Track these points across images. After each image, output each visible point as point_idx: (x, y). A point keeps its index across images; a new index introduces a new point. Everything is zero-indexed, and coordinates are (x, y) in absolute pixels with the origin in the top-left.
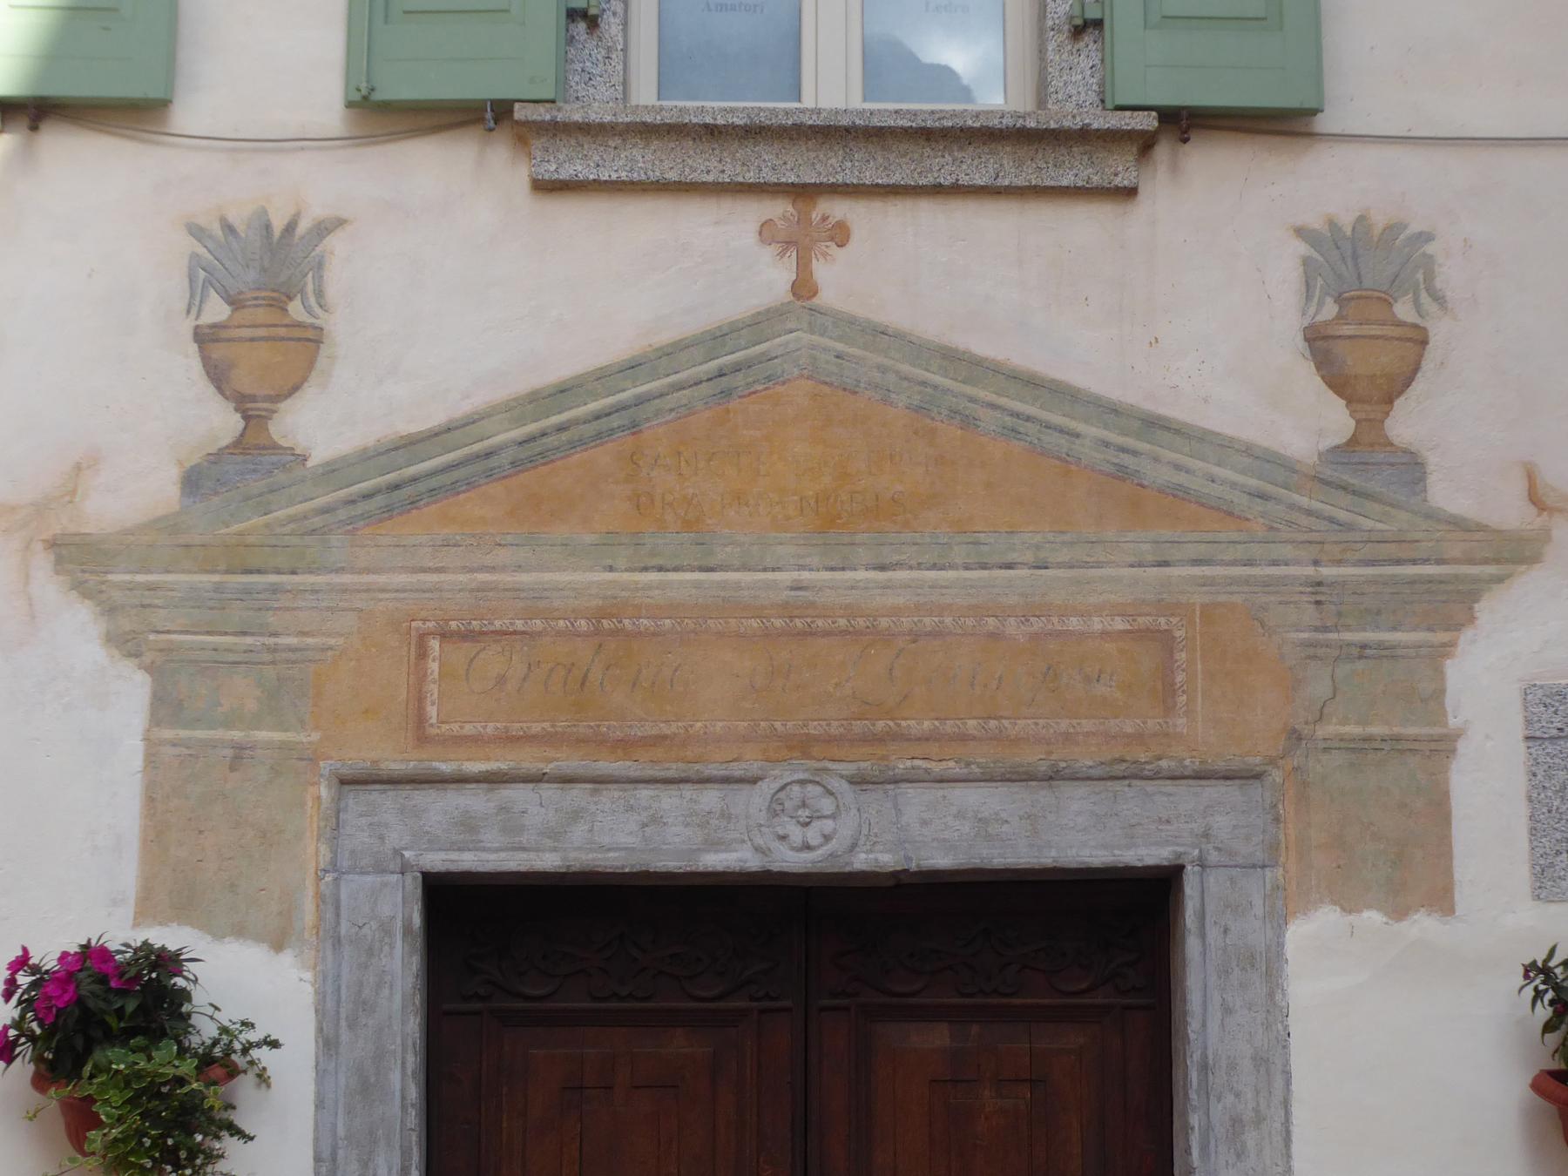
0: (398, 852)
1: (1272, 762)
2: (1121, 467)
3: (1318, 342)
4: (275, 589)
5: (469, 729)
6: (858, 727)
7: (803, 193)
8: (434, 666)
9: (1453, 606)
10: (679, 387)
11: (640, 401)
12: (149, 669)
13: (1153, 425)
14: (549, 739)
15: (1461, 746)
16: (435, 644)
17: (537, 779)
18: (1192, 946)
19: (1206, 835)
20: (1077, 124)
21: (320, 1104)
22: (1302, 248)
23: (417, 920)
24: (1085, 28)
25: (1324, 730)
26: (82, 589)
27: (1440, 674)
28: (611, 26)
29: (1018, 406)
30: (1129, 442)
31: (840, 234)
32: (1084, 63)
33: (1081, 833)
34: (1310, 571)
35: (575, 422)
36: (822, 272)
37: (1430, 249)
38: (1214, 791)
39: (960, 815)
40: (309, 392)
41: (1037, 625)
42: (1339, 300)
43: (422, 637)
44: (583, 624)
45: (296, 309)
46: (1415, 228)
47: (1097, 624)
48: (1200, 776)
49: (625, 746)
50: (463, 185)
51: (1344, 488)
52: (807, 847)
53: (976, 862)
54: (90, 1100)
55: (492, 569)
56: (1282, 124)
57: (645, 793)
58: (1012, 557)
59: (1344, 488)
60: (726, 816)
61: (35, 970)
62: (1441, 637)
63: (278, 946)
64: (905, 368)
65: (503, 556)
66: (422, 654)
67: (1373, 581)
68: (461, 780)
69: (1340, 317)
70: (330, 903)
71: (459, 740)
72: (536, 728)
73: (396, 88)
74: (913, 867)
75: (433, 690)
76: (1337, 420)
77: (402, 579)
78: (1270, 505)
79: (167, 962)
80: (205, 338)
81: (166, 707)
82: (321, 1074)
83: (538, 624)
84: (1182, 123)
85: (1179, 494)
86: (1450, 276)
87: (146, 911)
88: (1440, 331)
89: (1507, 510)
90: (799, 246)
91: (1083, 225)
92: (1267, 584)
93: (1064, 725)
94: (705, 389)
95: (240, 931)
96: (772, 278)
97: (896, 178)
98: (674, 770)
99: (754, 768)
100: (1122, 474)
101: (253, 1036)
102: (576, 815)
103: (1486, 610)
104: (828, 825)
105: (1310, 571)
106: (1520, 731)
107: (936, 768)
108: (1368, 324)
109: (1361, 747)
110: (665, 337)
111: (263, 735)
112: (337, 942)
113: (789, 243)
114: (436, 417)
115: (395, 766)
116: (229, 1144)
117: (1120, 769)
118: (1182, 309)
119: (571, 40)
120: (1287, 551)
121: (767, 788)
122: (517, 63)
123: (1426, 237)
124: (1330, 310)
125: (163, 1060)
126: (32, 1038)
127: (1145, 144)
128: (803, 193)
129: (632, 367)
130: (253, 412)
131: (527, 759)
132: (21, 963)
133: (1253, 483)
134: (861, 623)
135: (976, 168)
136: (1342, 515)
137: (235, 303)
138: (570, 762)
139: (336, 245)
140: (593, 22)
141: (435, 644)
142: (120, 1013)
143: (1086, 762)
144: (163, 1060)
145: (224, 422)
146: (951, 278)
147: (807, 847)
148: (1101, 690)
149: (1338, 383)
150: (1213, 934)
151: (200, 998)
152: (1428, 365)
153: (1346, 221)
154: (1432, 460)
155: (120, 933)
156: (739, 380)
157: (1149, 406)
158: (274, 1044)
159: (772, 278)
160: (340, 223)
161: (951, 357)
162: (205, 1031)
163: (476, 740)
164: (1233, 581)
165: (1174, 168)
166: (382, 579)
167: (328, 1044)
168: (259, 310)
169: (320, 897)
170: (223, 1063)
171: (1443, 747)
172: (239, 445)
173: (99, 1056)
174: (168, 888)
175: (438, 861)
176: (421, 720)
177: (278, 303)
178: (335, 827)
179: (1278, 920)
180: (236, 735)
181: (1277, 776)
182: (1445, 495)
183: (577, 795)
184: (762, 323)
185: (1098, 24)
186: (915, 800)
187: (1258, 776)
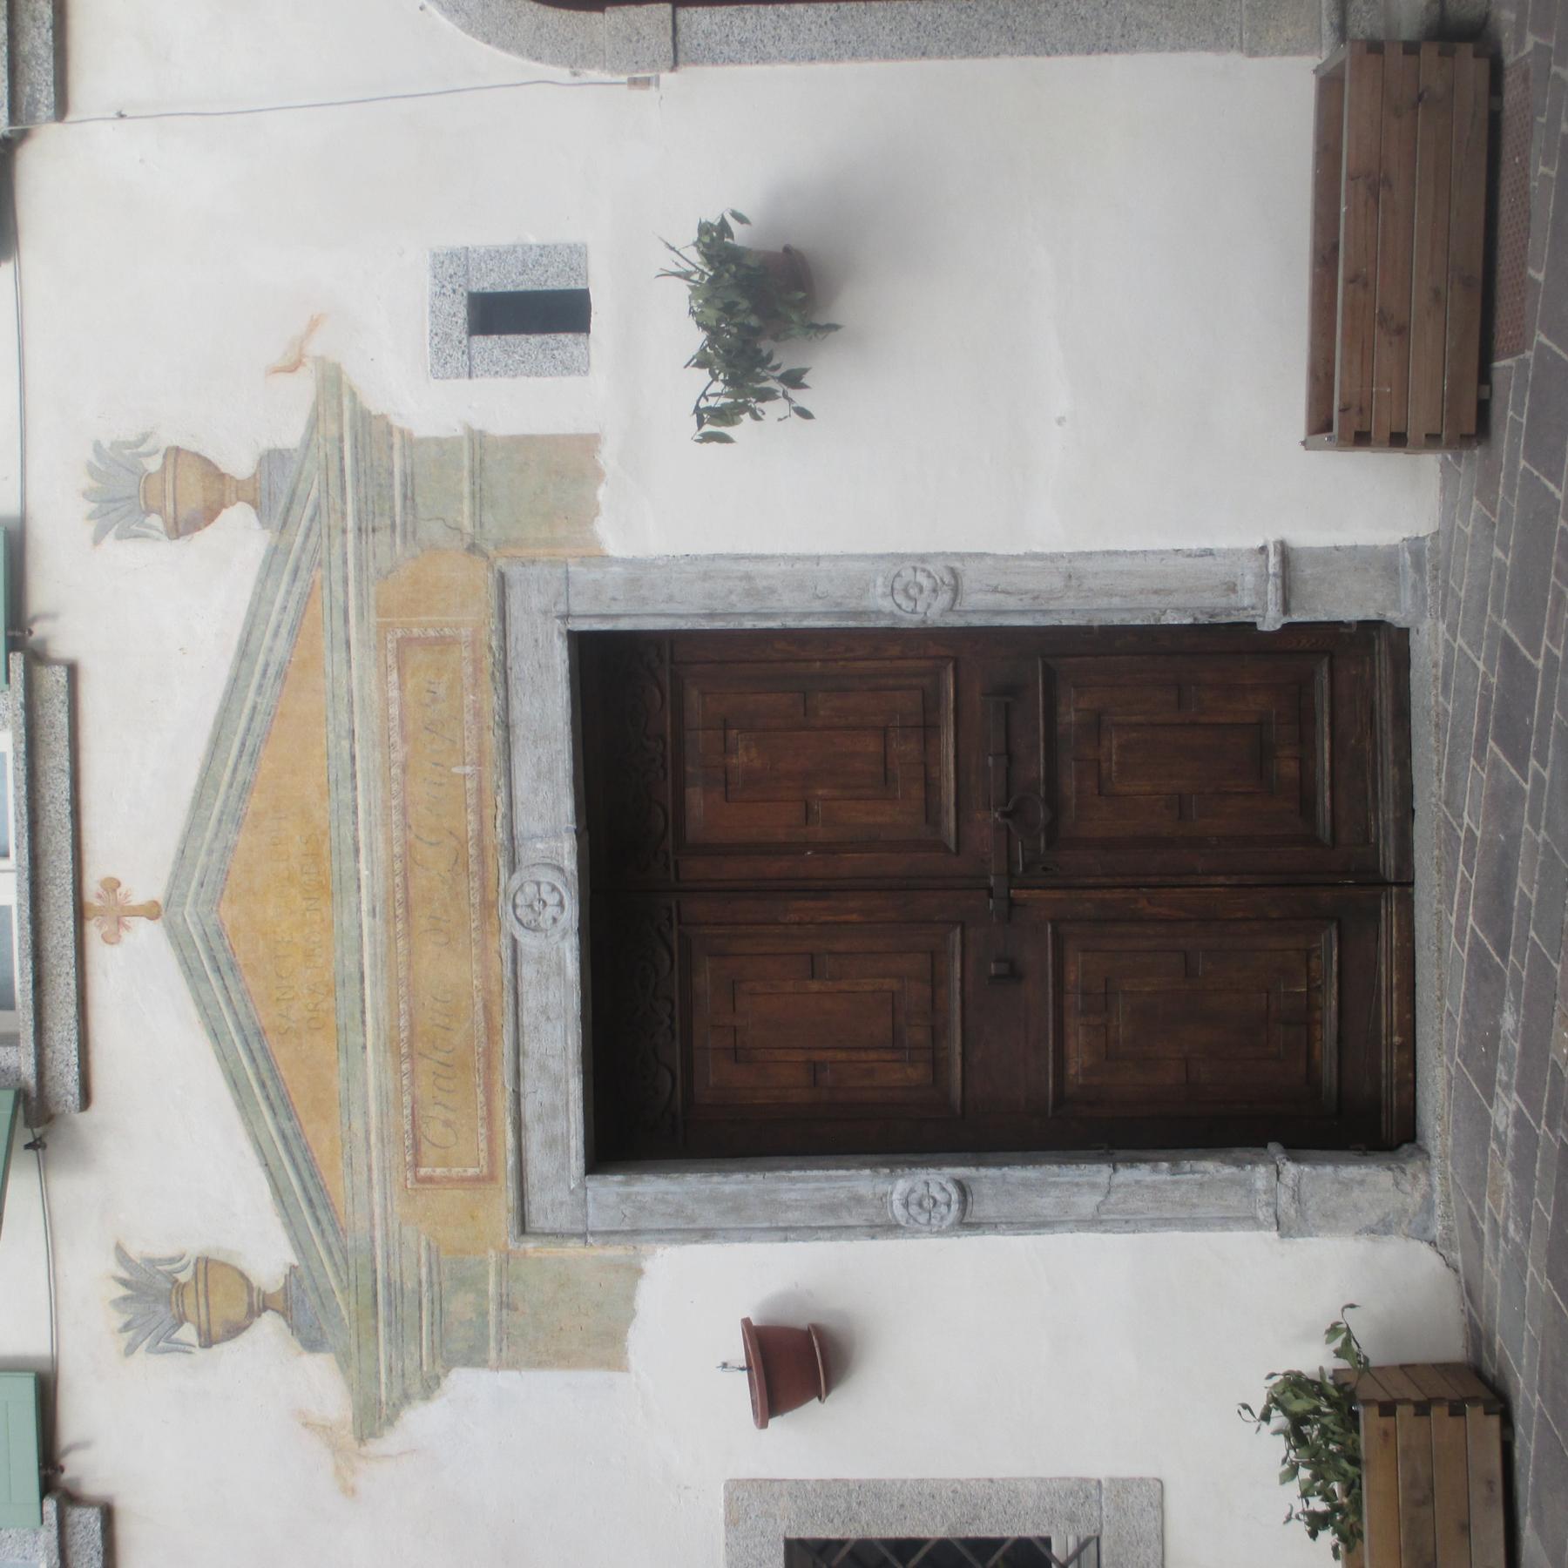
0: (572, 1192)
1: (491, 566)
2: (278, 674)
3: (180, 529)
5: (483, 1145)
6: (473, 867)
7: (80, 913)
8: (439, 1171)
9: (371, 432)
10: (229, 1001)
11: (240, 1027)
13: (245, 652)
14: (489, 1089)
15: (477, 426)
16: (423, 1171)
17: (517, 1096)
19: (545, 613)
22: (109, 539)
30: (259, 668)
31: (112, 885)
34: (350, 536)
36: (139, 898)
38: (514, 607)
39: (535, 791)
40: (243, 1265)
41: (396, 738)
42: (148, 511)
45: (184, 1277)
47: (394, 693)
49: (491, 1030)
51: (288, 510)
52: (561, 904)
55: (367, 1132)
57: (526, 1019)
58: (346, 756)
59: (288, 510)
60: (540, 960)
62: (397, 440)
63: (639, 1272)
64: (209, 835)
65: (357, 1125)
66: (430, 1180)
69: (160, 512)
71: (491, 1153)
72: (481, 1098)
74: (573, 826)
75: (456, 1171)
76: (237, 516)
78: (304, 566)
80: (208, 1341)
81: (474, 1357)
83: (407, 1099)
85: (295, 631)
89: (302, 389)
90: (121, 915)
92: (360, 568)
93: (468, 717)
94: (230, 981)
95: (629, 1299)
96: (144, 933)
97: (66, 845)
98: (508, 998)
100: (282, 674)
102: (543, 1068)
103: (375, 405)
104: (545, 888)
105: (350, 536)
106: (464, 382)
107: (502, 809)
108: (169, 493)
110: (193, 1012)
111: (492, 1288)
113: (119, 922)
115: (509, 1197)
120: (336, 551)
124: (155, 520)
127: (36, 658)
128: (80, 913)
129: (215, 1035)
130: (260, 1304)
131: (504, 1103)
133: (286, 578)
134: (398, 866)
136: (309, 512)
137: (181, 1320)
139: (135, 1250)
141: (423, 1171)
143: (492, 702)
145: (269, 1325)
148: (441, 691)
149: (209, 514)
150: (616, 609)
152: (194, 447)
153: (91, 507)
154: (266, 444)
156: (221, 957)
159: (144, 933)
160: (119, 1249)
161: (200, 800)
163: (491, 1140)
164: (360, 594)
166: (378, 1211)
168: (183, 1302)
171: (478, 440)
172: (285, 1313)
175: (577, 1163)
176: (477, 1179)
177: (180, 1288)
180: (492, 1307)
181: (501, 563)
182: (291, 435)
183: (528, 1067)
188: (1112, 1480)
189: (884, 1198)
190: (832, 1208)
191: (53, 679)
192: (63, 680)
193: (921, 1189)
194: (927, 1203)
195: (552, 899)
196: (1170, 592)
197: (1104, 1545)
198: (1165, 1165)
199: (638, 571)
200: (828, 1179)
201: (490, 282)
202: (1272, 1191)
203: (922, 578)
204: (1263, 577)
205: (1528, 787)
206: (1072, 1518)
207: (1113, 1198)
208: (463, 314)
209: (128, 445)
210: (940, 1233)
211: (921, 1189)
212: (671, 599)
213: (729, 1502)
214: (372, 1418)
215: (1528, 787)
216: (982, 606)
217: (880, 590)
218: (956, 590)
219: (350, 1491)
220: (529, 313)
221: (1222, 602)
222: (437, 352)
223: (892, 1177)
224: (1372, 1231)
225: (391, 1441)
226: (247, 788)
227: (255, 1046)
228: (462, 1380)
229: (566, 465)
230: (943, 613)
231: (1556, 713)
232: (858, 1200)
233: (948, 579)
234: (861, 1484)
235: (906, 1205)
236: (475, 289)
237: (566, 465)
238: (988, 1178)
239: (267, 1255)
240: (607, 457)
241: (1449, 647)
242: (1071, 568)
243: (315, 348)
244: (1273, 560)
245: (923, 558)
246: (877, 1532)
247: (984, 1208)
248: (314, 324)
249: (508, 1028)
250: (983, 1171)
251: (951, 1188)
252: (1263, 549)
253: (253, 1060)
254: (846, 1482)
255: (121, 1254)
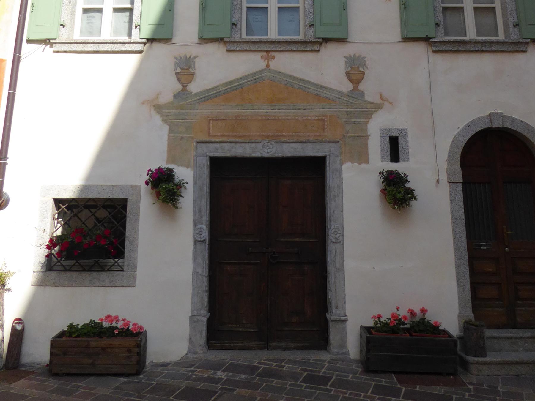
1: (340, 139)
2: (317, 94)
3: (348, 74)
4: (187, 113)
8: (211, 125)
9: (368, 115)
10: (248, 81)
11: (243, 83)
12: (169, 125)
13: (322, 87)
14: (229, 136)
17: (227, 142)
18: (328, 168)
19: (330, 151)
20: (310, 40)
21: (194, 191)
22: (345, 59)
23: (209, 164)
24: (311, 25)
25: (348, 135)
26: (159, 113)
27: (367, 126)
28: (239, 26)
29: (300, 84)
30: (319, 90)
31: (274, 58)
32: (311, 31)
33: (311, 151)
34: (346, 110)
35: (233, 87)
36: (271, 63)
37: (365, 59)
38: (331, 144)
39: (292, 148)
40: (193, 82)
41: (304, 118)
42: (351, 67)
43: (209, 120)
44: (234, 118)
45: (191, 70)
46: (363, 56)
47: (313, 118)
48: (329, 142)
49: (240, 137)
50: (216, 51)
51: (351, 97)
52: (268, 153)
53: (294, 155)
54: (160, 191)
55: (220, 110)
56: (342, 40)
57: (243, 144)
59: (351, 97)
60: (256, 148)
61: (151, 171)
62: (367, 120)
63: (188, 168)
66: (209, 123)
67: (356, 111)
68: (215, 142)
69: (351, 70)
70: (195, 161)
71: (215, 136)
72: (227, 134)
73: (206, 36)
76: (350, 86)
77: (206, 111)
78: (340, 100)
79: (171, 170)
80: (177, 74)
81: (171, 131)
82: (194, 187)
83: (227, 118)
84: (326, 40)
85: (326, 98)
86: (368, 63)
87: (168, 162)
88: (367, 72)
89: (377, 100)
90: (267, 59)
91: (311, 56)
92: (340, 112)
93: (308, 134)
94: (253, 82)
96: (263, 64)
97: (282, 49)
98: (248, 141)
99: (260, 140)
100: (317, 95)
101: (184, 182)
102: (233, 148)
103: (373, 116)
104: (271, 149)
105: (346, 110)
106: (379, 135)
108: (355, 72)
109: (354, 137)
110: (247, 74)
111: (185, 135)
112: (196, 167)
113: (266, 59)
114: (212, 87)
115: (205, 140)
116: (180, 198)
117: (316, 141)
118: (326, 69)
119: (232, 28)
121: (262, 144)
122: (224, 33)
123: (365, 58)
124: (350, 69)
125: (171, 186)
126: (151, 182)
127: (320, 44)
128: (268, 51)
129: (241, 78)
130: (184, 85)
132: (149, 170)
133: (337, 96)
134: (276, 118)
135: (294, 47)
136: (351, 101)
137: (181, 69)
138: (232, 139)
139: (197, 60)
140: (236, 25)
142: (164, 178)
143: (311, 139)
144: (171, 186)
145: (180, 87)
146: (290, 64)
147: (268, 153)
149: (351, 80)
150: (331, 166)
151: (176, 176)
152: (365, 77)
153: (352, 55)
154: (365, 92)
155: (164, 166)
156: (258, 80)
157: (321, 84)
158: (187, 183)
159: (263, 64)
160: (197, 56)
161: (290, 76)
162: (177, 181)
163: (218, 136)
165: (325, 47)
166: (203, 111)
167: (195, 182)
168: (185, 70)
169: (194, 160)
170: (180, 186)
171: (367, 137)
173: (161, 185)
174: (171, 159)
175: (212, 155)
176: (209, 133)
178: (196, 150)
179: (341, 164)
180: (181, 135)
181: (341, 142)
182: (368, 98)
183: (233, 144)
184: (261, 72)
185: (313, 25)
186: (285, 146)
187: (338, 142)
188: (136, 275)
189: (201, 223)
190: (200, 211)
191: (316, 47)
192: (316, 49)
193: (204, 232)
194: (201, 233)
195: (269, 151)
196: (336, 293)
197: (121, 272)
198: (207, 289)
199: (340, 171)
200: (206, 210)
201: (401, 141)
202: (200, 314)
203: (338, 235)
204: (339, 315)
205: (298, 383)
206: (128, 265)
207: (200, 276)
208: (394, 135)
209: (365, 64)
210: (194, 236)
211: (204, 232)
212: (333, 178)
213: (136, 186)
214: (158, 108)
215: (298, 383)
216: (332, 248)
217: (336, 225)
218: (336, 243)
219: (143, 103)
220: (394, 148)
221: (333, 305)
222: (386, 129)
223: (206, 225)
224: (190, 339)
225: (153, 112)
226: (293, 87)
227: (239, 87)
228: (166, 128)
229: (362, 156)
230: (331, 240)
231: (318, 392)
232: (201, 217)
233: (338, 241)
234: (139, 216)
235: (200, 228)
236: (399, 138)
237: (362, 156)
238: (206, 247)
239: (195, 87)
240: (364, 165)
241: (325, 361)
242: (341, 269)
243: (386, 103)
244: (343, 318)
245: (343, 235)
246: (128, 219)
247: (199, 246)
248: (391, 103)
249: (241, 141)
250: (207, 246)
251: (204, 239)
252: (346, 316)
253: (236, 86)
254: (139, 213)
255: (195, 57)
